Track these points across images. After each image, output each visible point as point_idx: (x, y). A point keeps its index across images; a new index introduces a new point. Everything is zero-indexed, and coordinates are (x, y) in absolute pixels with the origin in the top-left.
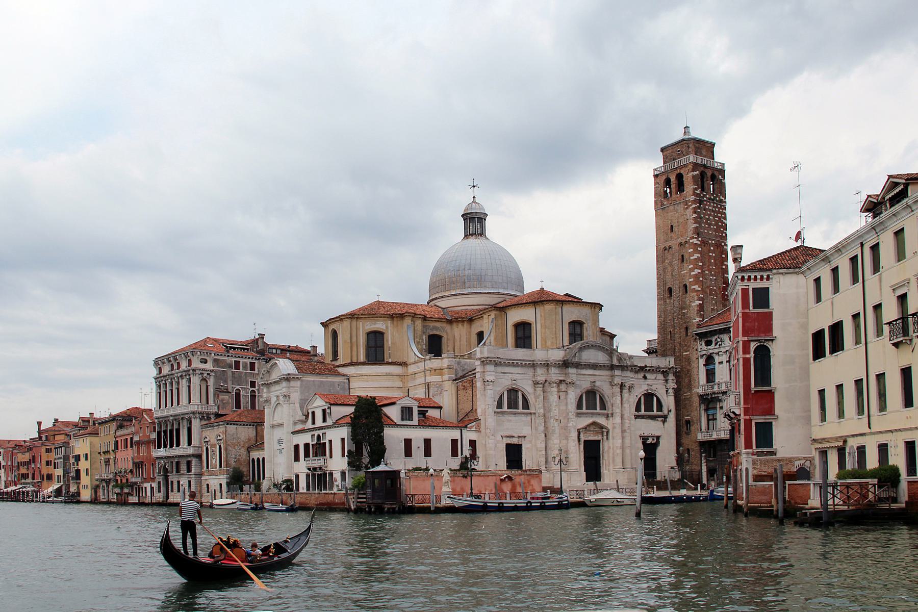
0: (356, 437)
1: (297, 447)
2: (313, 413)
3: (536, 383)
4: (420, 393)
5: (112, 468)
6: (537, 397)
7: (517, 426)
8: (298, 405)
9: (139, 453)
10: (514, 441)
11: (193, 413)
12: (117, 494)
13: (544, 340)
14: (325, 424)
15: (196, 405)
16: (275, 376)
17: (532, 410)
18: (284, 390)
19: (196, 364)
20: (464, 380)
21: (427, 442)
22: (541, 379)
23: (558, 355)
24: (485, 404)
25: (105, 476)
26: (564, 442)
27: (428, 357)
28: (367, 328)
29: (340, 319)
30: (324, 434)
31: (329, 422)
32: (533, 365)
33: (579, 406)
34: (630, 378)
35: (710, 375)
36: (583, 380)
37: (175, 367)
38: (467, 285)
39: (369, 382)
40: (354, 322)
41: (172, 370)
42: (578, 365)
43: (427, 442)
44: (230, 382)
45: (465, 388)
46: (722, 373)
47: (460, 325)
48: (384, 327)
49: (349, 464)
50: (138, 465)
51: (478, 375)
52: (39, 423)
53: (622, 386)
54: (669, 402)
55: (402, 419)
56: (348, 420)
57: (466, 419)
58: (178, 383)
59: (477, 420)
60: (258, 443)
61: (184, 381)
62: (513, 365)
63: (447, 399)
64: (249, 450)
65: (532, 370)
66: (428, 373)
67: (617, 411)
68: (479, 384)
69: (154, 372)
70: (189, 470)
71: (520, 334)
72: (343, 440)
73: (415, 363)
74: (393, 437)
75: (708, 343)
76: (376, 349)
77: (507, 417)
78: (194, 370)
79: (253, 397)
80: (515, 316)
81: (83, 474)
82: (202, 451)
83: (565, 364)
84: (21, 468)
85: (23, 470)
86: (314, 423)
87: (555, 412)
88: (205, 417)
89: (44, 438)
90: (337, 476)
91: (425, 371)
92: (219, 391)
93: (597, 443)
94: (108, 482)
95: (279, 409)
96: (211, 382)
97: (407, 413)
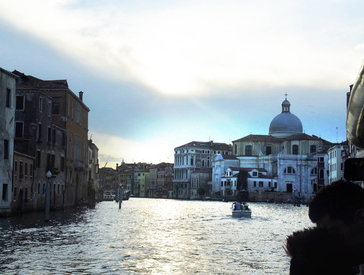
0: (238, 180)
1: (222, 182)
2: (227, 173)
3: (297, 165)
4: (261, 166)
5: (155, 185)
6: (297, 170)
7: (291, 178)
8: (223, 169)
9: (167, 180)
10: (290, 183)
11: (188, 168)
12: (157, 195)
13: (302, 152)
14: (230, 176)
15: (189, 165)
16: (217, 159)
17: (296, 174)
18: (219, 164)
19: (190, 151)
20: (274, 163)
22: (299, 164)
23: (305, 157)
24: (280, 172)
25: (151, 188)
26: (306, 184)
27: (264, 155)
28: (246, 145)
29: (237, 141)
30: (230, 179)
32: (296, 160)
33: (312, 172)
37: (182, 152)
38: (281, 130)
39: (246, 162)
40: (242, 143)
41: (181, 153)
42: (311, 160)
44: (201, 158)
45: (275, 166)
47: (277, 144)
48: (252, 144)
49: (237, 188)
51: (278, 163)
52: (117, 164)
55: (253, 176)
56: (237, 176)
57: (274, 175)
58: (183, 157)
59: (277, 176)
61: (185, 157)
62: (290, 160)
63: (269, 168)
64: (207, 181)
65: (296, 162)
66: (264, 160)
68: (278, 165)
69: (174, 153)
70: (186, 187)
71: (295, 149)
72: (235, 181)
73: (261, 156)
74: (251, 180)
76: (249, 152)
77: (287, 176)
78: (189, 154)
79: (208, 162)
80: (294, 143)
81: (141, 186)
82: (191, 181)
83: (307, 160)
84: (107, 182)
85: (108, 184)
86: (227, 175)
87: (304, 174)
88: (191, 169)
89: (119, 171)
90: (233, 191)
91: (263, 159)
92: (197, 160)
94: (153, 190)
95: (217, 169)
96: (194, 158)
97: (255, 174)
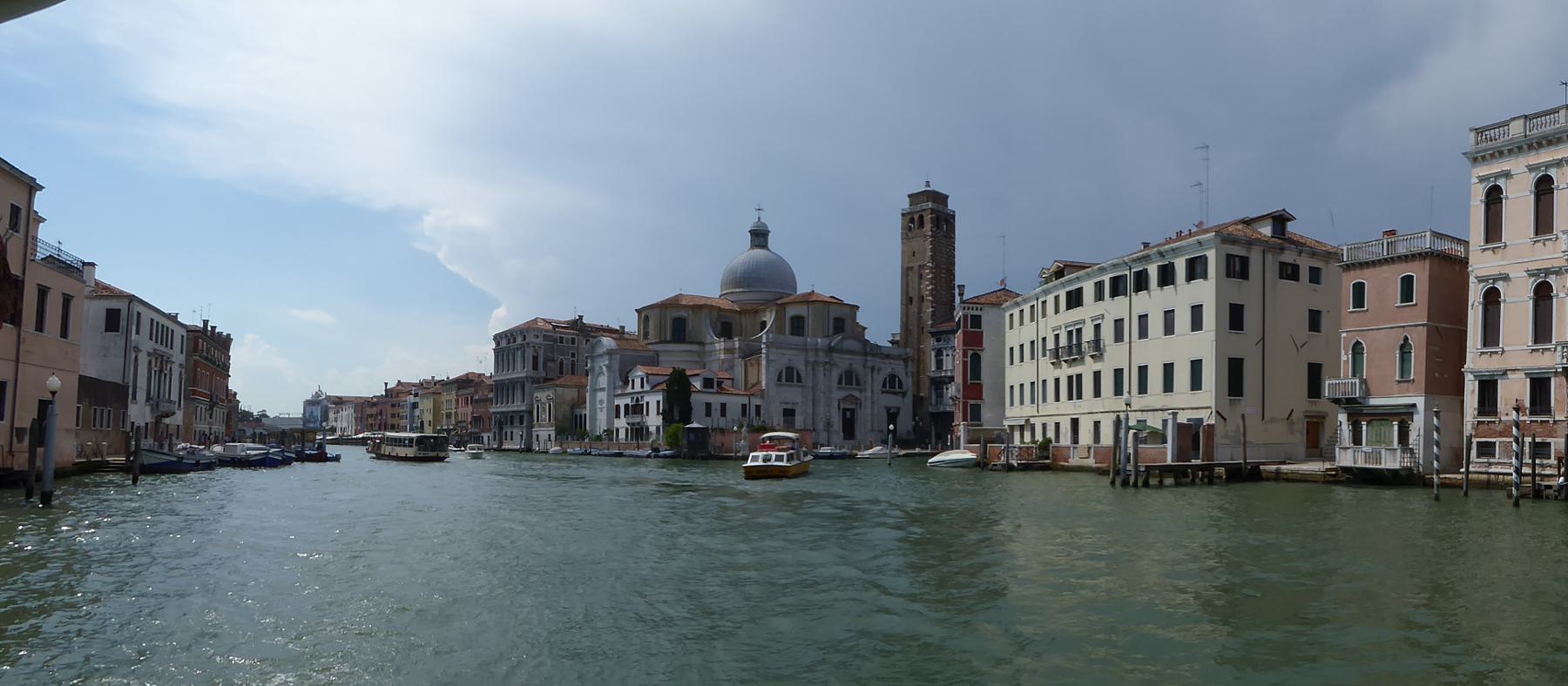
0: (668, 400)
3: (807, 363)
16: (600, 351)
21: (723, 406)
22: (812, 359)
31: (647, 388)
33: (840, 382)
34: (878, 362)
35: (939, 364)
36: (843, 362)
42: (840, 351)
43: (723, 406)
46: (948, 364)
50: (477, 420)
53: (873, 369)
54: (908, 382)
60: (581, 402)
67: (869, 387)
74: (698, 400)
75: (938, 340)
80: (791, 311)
83: (830, 350)
88: (535, 381)
90: (652, 429)
93: (852, 411)
